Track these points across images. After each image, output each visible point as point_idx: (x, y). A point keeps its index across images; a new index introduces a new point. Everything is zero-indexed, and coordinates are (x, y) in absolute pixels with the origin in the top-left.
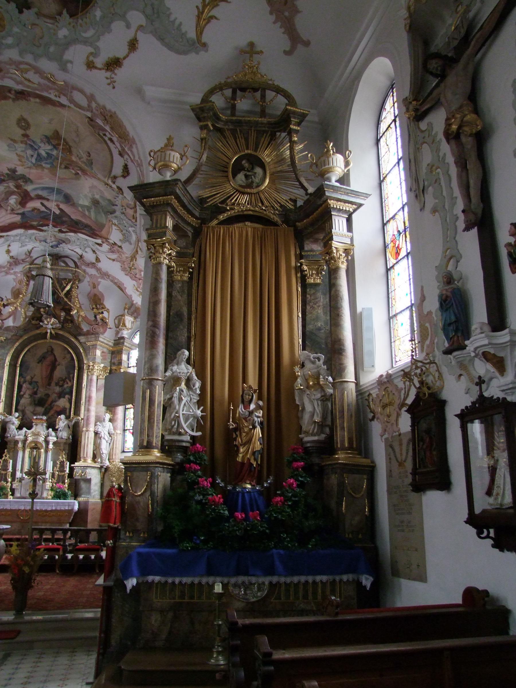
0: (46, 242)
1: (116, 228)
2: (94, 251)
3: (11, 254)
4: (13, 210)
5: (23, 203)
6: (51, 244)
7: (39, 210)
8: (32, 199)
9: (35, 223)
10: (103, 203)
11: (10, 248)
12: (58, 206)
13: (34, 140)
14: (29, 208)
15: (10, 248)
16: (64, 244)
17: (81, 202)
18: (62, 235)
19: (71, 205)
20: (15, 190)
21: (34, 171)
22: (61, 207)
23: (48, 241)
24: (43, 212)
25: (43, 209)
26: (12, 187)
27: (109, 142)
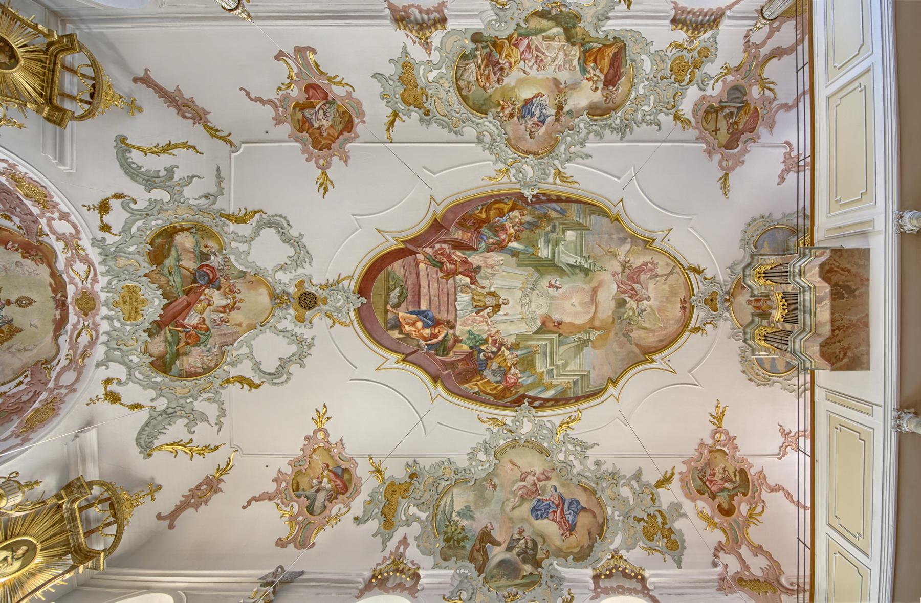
27: (17, 381)
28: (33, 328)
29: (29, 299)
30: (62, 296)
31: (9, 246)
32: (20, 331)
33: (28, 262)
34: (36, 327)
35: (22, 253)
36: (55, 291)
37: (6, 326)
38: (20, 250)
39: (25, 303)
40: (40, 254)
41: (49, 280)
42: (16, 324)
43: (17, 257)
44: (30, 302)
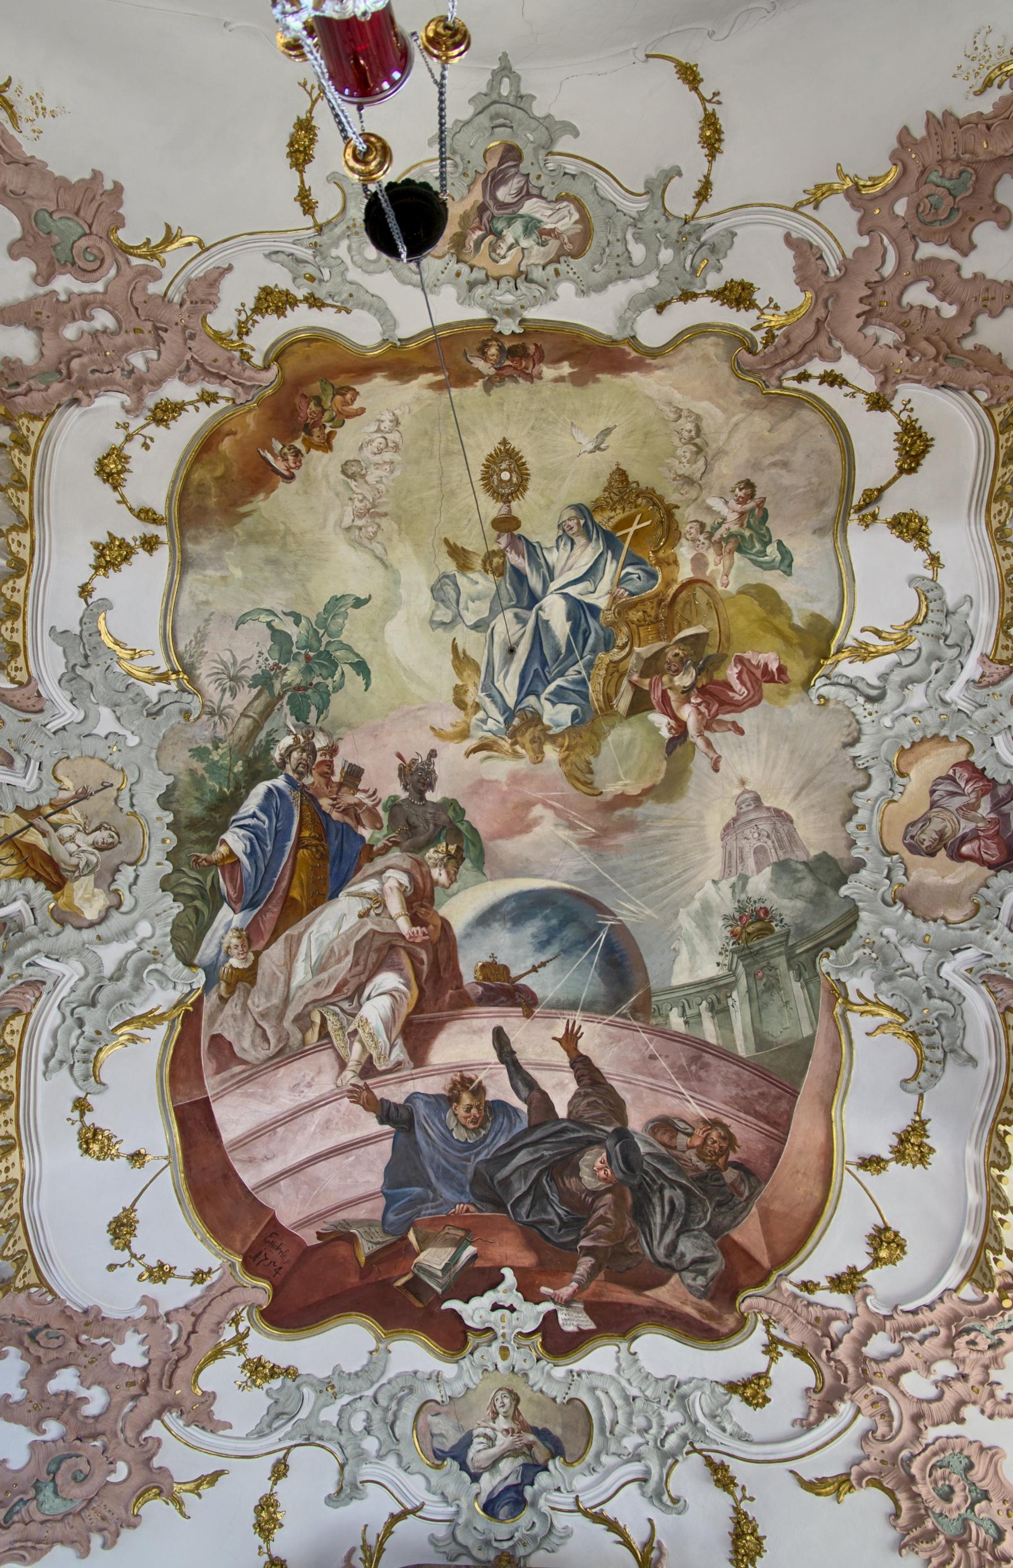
0: (464, 1467)
1: (869, 1022)
2: (722, 1477)
3: (282, 1544)
4: (368, 1069)
5: (417, 1033)
6: (488, 1483)
7: (479, 1091)
8: (463, 1002)
9: (435, 1258)
10: (788, 908)
11: (283, 1490)
12: (570, 1040)
13: (533, 539)
14: (439, 1072)
15: (283, 1490)
16: (556, 1465)
17: (680, 977)
18: (552, 1378)
19: (635, 1011)
20: (404, 925)
21: (500, 769)
22: (584, 1046)
23: (478, 1453)
24: (500, 1107)
25: (500, 1087)
26: (395, 905)
28: (610, 440)
29: (492, 463)
30: (483, 353)
31: (280, 466)
32: (621, 475)
33: (348, 438)
34: (607, 432)
35: (310, 446)
36: (463, 378)
37: (598, 518)
38: (298, 444)
39: (506, 473)
40: (315, 388)
41: (418, 386)
42: (590, 493)
43: (321, 465)
44: (507, 455)
